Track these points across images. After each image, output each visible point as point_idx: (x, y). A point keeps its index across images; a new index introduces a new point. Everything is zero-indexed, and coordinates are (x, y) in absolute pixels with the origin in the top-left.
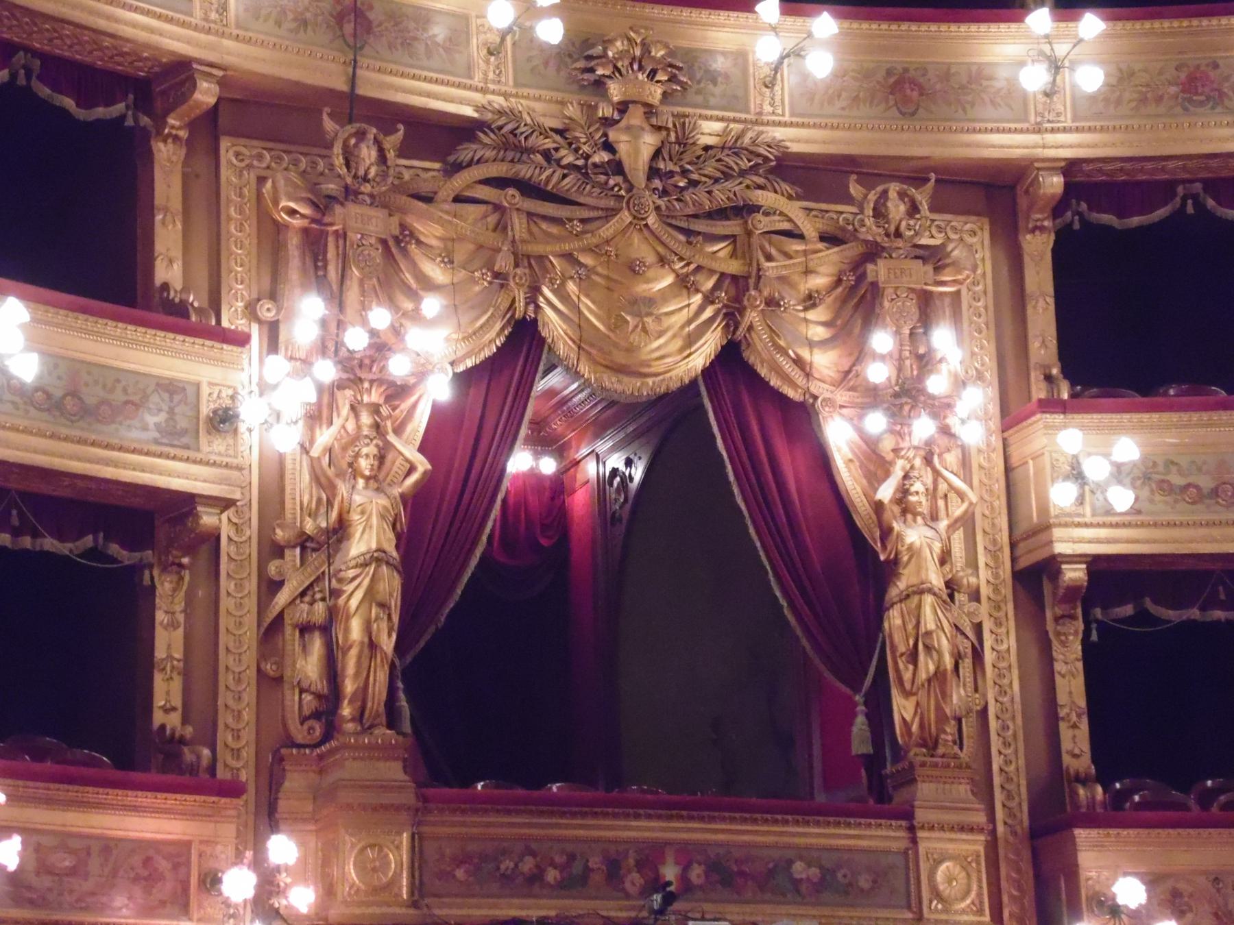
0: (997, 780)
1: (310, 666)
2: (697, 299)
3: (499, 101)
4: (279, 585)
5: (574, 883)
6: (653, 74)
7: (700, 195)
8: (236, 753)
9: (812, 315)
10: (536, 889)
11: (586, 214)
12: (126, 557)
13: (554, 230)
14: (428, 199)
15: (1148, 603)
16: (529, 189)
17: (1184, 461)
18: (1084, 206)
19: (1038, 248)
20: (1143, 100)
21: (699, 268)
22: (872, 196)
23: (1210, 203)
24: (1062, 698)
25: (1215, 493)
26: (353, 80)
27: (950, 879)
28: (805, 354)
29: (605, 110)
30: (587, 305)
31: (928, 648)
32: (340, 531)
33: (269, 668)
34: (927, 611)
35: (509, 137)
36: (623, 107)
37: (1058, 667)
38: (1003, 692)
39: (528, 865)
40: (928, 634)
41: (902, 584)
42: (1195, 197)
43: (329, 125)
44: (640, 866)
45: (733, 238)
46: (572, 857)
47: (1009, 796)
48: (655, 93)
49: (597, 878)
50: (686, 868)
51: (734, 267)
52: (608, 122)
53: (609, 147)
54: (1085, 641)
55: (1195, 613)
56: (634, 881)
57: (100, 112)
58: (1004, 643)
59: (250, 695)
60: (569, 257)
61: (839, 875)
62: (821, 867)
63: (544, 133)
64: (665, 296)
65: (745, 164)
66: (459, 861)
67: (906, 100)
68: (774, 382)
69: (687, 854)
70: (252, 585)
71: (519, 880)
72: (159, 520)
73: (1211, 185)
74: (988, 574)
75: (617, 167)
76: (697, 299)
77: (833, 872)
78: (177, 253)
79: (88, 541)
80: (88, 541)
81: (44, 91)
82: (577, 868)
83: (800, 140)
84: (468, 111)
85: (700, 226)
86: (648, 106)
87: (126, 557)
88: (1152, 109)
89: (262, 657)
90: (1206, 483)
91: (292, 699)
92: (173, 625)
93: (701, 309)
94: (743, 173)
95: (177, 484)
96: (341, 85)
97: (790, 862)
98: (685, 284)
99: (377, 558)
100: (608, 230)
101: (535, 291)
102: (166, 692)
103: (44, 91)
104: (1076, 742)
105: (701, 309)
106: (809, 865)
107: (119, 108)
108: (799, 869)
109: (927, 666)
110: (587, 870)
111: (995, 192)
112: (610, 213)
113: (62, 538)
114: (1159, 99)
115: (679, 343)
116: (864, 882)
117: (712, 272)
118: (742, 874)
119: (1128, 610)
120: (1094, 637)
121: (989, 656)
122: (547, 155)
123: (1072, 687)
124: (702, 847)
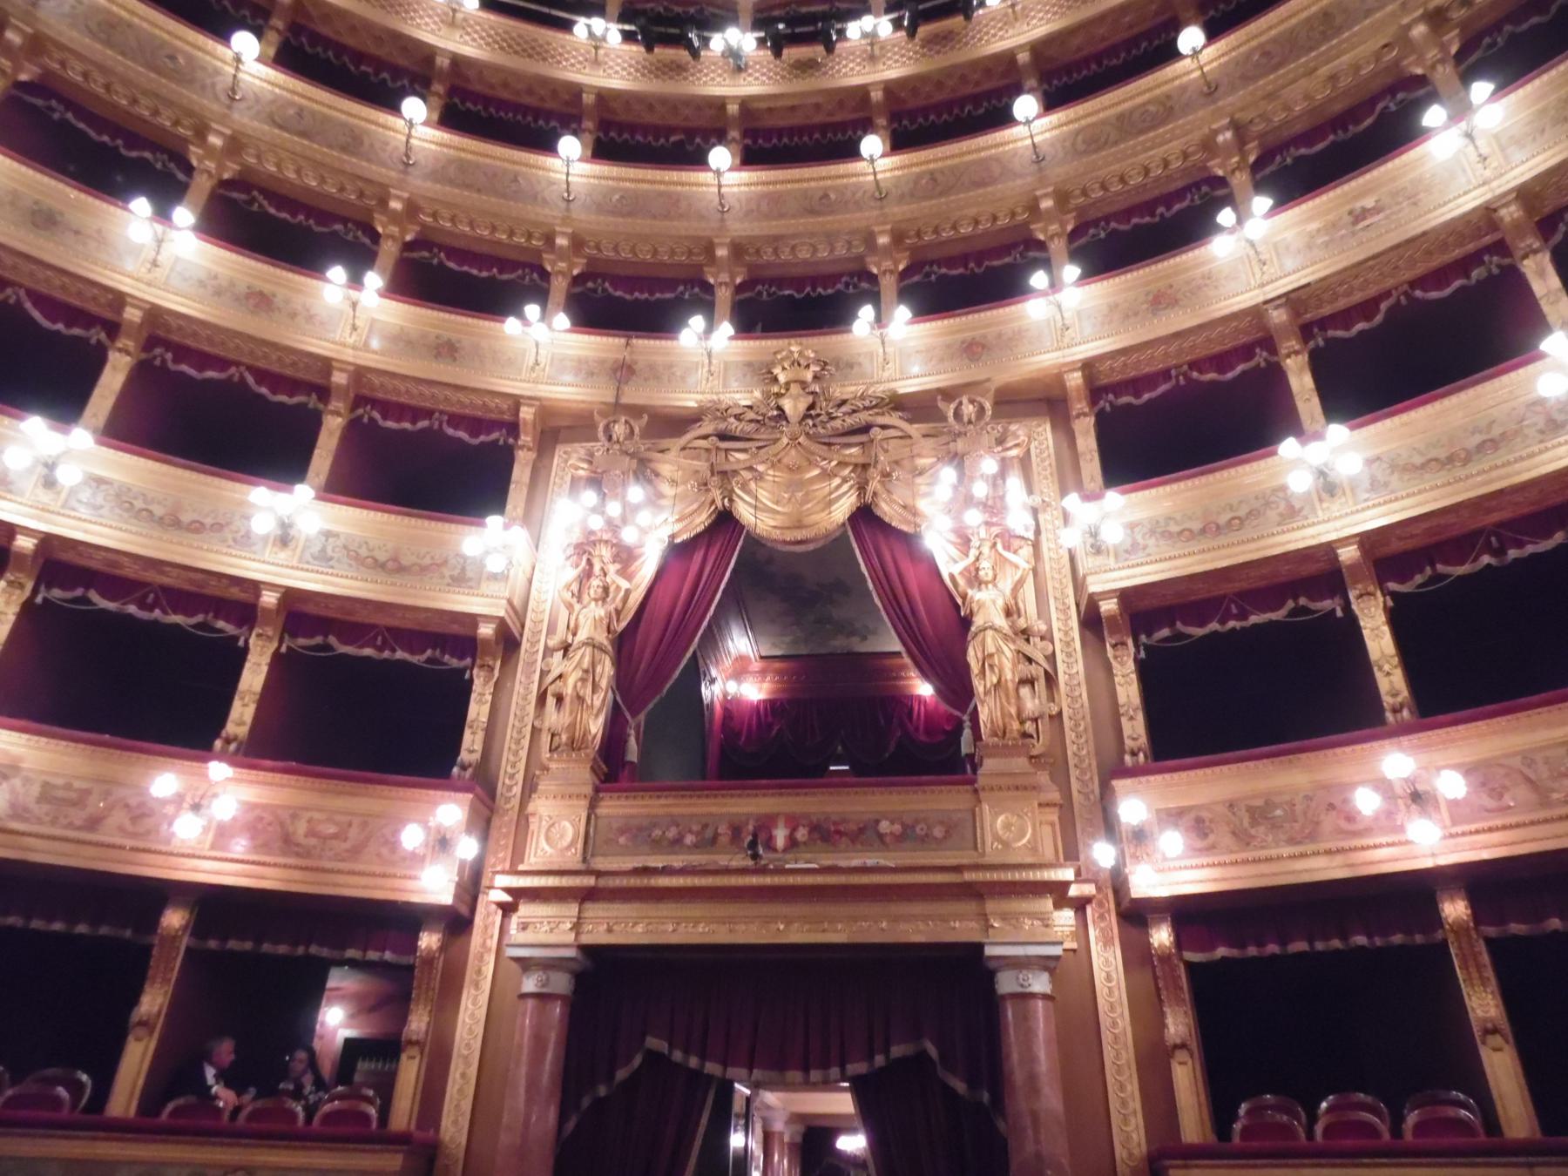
0: (1071, 762)
2: (837, 481)
5: (708, 842)
6: (808, 366)
7: (837, 424)
8: (512, 777)
12: (455, 663)
15: (1179, 625)
16: (723, 436)
17: (1178, 516)
18: (1111, 396)
20: (1127, 317)
21: (840, 463)
22: (953, 406)
23: (1195, 374)
24: (1122, 699)
25: (1203, 531)
27: (1007, 826)
29: (776, 389)
30: (764, 496)
31: (991, 666)
34: (989, 641)
35: (721, 412)
36: (788, 384)
39: (672, 833)
40: (991, 655)
46: (705, 826)
47: (1083, 772)
48: (809, 376)
49: (724, 840)
50: (794, 830)
51: (861, 460)
52: (779, 395)
53: (779, 408)
54: (1136, 660)
55: (1214, 626)
57: (482, 438)
58: (1072, 666)
60: (750, 469)
61: (918, 829)
62: (903, 824)
64: (812, 480)
66: (622, 831)
71: (665, 843)
73: (1193, 365)
74: (1065, 626)
75: (782, 415)
77: (913, 827)
81: (450, 431)
82: (709, 833)
83: (906, 387)
87: (455, 663)
89: (536, 717)
90: (1196, 526)
91: (545, 739)
92: (480, 702)
97: (877, 822)
98: (827, 475)
99: (591, 643)
103: (450, 431)
104: (1135, 729)
106: (892, 823)
107: (494, 436)
108: (884, 826)
109: (992, 679)
113: (412, 653)
114: (1136, 314)
115: (821, 506)
116: (938, 832)
118: (838, 832)
119: (1165, 632)
120: (1143, 655)
121: (1062, 678)
123: (1128, 691)
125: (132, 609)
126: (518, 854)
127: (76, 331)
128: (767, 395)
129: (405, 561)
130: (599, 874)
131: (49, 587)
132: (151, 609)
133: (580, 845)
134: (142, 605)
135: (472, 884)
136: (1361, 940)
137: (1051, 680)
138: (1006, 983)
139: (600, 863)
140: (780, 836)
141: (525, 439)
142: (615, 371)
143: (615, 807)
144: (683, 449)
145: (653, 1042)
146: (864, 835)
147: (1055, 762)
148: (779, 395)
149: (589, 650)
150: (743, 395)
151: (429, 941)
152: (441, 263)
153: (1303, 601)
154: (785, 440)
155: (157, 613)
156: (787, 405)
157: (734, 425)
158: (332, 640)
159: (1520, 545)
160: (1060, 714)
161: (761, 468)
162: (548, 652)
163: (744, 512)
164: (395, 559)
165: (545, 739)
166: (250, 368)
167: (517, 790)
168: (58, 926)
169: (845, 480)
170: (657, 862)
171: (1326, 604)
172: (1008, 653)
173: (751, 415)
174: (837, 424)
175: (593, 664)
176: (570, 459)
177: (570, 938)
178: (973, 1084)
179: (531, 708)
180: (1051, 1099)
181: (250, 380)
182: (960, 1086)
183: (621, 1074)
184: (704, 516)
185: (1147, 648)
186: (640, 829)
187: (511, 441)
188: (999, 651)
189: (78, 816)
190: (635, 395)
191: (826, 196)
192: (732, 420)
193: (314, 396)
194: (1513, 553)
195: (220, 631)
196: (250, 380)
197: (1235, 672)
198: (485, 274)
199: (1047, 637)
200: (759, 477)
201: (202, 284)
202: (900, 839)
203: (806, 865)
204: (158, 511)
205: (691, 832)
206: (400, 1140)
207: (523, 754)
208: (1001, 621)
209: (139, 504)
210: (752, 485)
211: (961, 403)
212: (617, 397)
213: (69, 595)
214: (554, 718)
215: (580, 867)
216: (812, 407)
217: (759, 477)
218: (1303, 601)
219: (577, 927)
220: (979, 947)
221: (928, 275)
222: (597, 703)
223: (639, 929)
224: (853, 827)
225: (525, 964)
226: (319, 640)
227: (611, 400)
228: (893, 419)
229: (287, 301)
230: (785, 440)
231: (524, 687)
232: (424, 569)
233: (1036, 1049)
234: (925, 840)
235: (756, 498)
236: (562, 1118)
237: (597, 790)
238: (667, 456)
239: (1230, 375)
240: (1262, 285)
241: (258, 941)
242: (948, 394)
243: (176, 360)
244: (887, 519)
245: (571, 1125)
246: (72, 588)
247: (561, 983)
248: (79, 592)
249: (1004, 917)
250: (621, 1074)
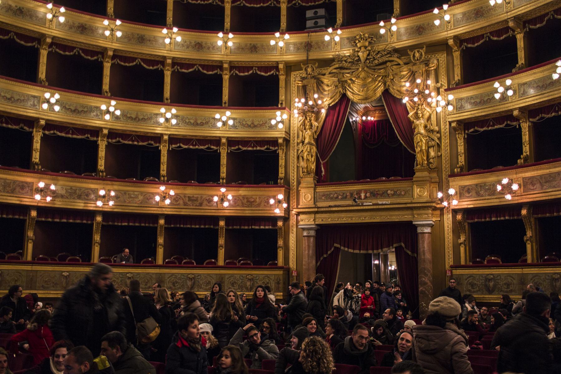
3: (337, 53)
5: (344, 198)
6: (366, 40)
7: (376, 62)
8: (293, 180)
12: (273, 148)
13: (348, 75)
14: (324, 75)
16: (341, 68)
19: (457, 55)
20: (468, 19)
24: (459, 151)
25: (480, 102)
27: (420, 191)
28: (399, 89)
29: (357, 50)
30: (355, 89)
36: (360, 48)
38: (446, 151)
39: (335, 196)
40: (419, 142)
42: (488, 37)
43: (302, 66)
44: (357, 194)
45: (384, 68)
48: (367, 44)
49: (348, 197)
50: (366, 194)
54: (464, 138)
55: (485, 129)
57: (269, 74)
58: (445, 142)
60: (351, 80)
63: (345, 56)
64: (369, 83)
65: (386, 53)
66: (323, 196)
67: (420, 31)
69: (366, 191)
75: (359, 60)
79: (266, 147)
80: (266, 147)
81: (259, 73)
82: (345, 195)
85: (375, 68)
87: (273, 148)
88: (469, 21)
91: (301, 169)
92: (282, 159)
93: (378, 84)
94: (386, 55)
98: (374, 80)
99: (309, 143)
102: (282, 171)
104: (462, 160)
105: (378, 84)
107: (272, 72)
108: (389, 192)
111: (441, 46)
113: (261, 147)
114: (470, 18)
116: (403, 193)
117: (380, 76)
119: (472, 130)
122: (345, 61)
123: (461, 148)
124: (369, 190)
125: (191, 147)
126: (298, 204)
127: (155, 67)
128: (354, 50)
129: (256, 123)
130: (318, 208)
131: (171, 145)
132: (195, 145)
133: (313, 200)
134: (193, 145)
135: (288, 211)
137: (439, 146)
138: (419, 230)
139: (320, 204)
140: (363, 195)
141: (281, 72)
142: (306, 46)
143: (320, 189)
144: (330, 73)
145: (336, 245)
146: (384, 194)
147: (438, 170)
148: (358, 52)
149: (309, 146)
150: (347, 52)
151: (280, 224)
152: (244, 5)
153: (509, 122)
154: (360, 69)
155: (197, 147)
156: (360, 54)
157: (345, 65)
158: (240, 147)
160: (441, 155)
161: (354, 79)
162: (298, 144)
163: (349, 94)
164: (253, 123)
165: (301, 169)
166: (200, 65)
167: (295, 183)
168: (197, 226)
169: (379, 82)
170: (332, 203)
171: (514, 123)
172: (424, 141)
173: (349, 60)
174: (376, 62)
175: (311, 150)
176: (296, 80)
177: (313, 223)
178: (413, 252)
179: (296, 160)
180: (428, 256)
181: (201, 69)
182: (410, 253)
183: (329, 252)
184: (338, 95)
185: (467, 134)
186: (327, 195)
187: (277, 73)
188: (421, 140)
189: (197, 203)
190: (314, 55)
192: (344, 62)
193: (219, 70)
195: (213, 149)
196: (201, 69)
197: (489, 144)
198: (258, 6)
199: (439, 132)
200: (353, 82)
201: (183, 46)
202: (393, 195)
203: (368, 204)
204: (192, 121)
206: (281, 268)
207: (295, 173)
208: (422, 131)
209: (187, 121)
210: (351, 85)
211: (415, 53)
212: (307, 57)
213: (176, 146)
214: (303, 164)
215: (313, 206)
216: (368, 55)
217: (353, 82)
218: (509, 122)
219: (314, 220)
220: (411, 222)
222: (313, 159)
223: (329, 220)
224: (381, 192)
225: (303, 229)
226: (237, 147)
227: (305, 58)
228: (395, 58)
229: (206, 44)
230: (360, 69)
231: (293, 154)
232: (261, 125)
233: (425, 245)
234: (400, 195)
235: (353, 90)
236: (317, 262)
237: (315, 185)
238: (325, 77)
239: (502, 38)
240: (507, 12)
241: (240, 226)
242: (412, 48)
243: (181, 68)
244: (393, 94)
245: (319, 264)
246: (177, 144)
247: (312, 233)
248: (178, 145)
249: (418, 215)
250: (329, 252)
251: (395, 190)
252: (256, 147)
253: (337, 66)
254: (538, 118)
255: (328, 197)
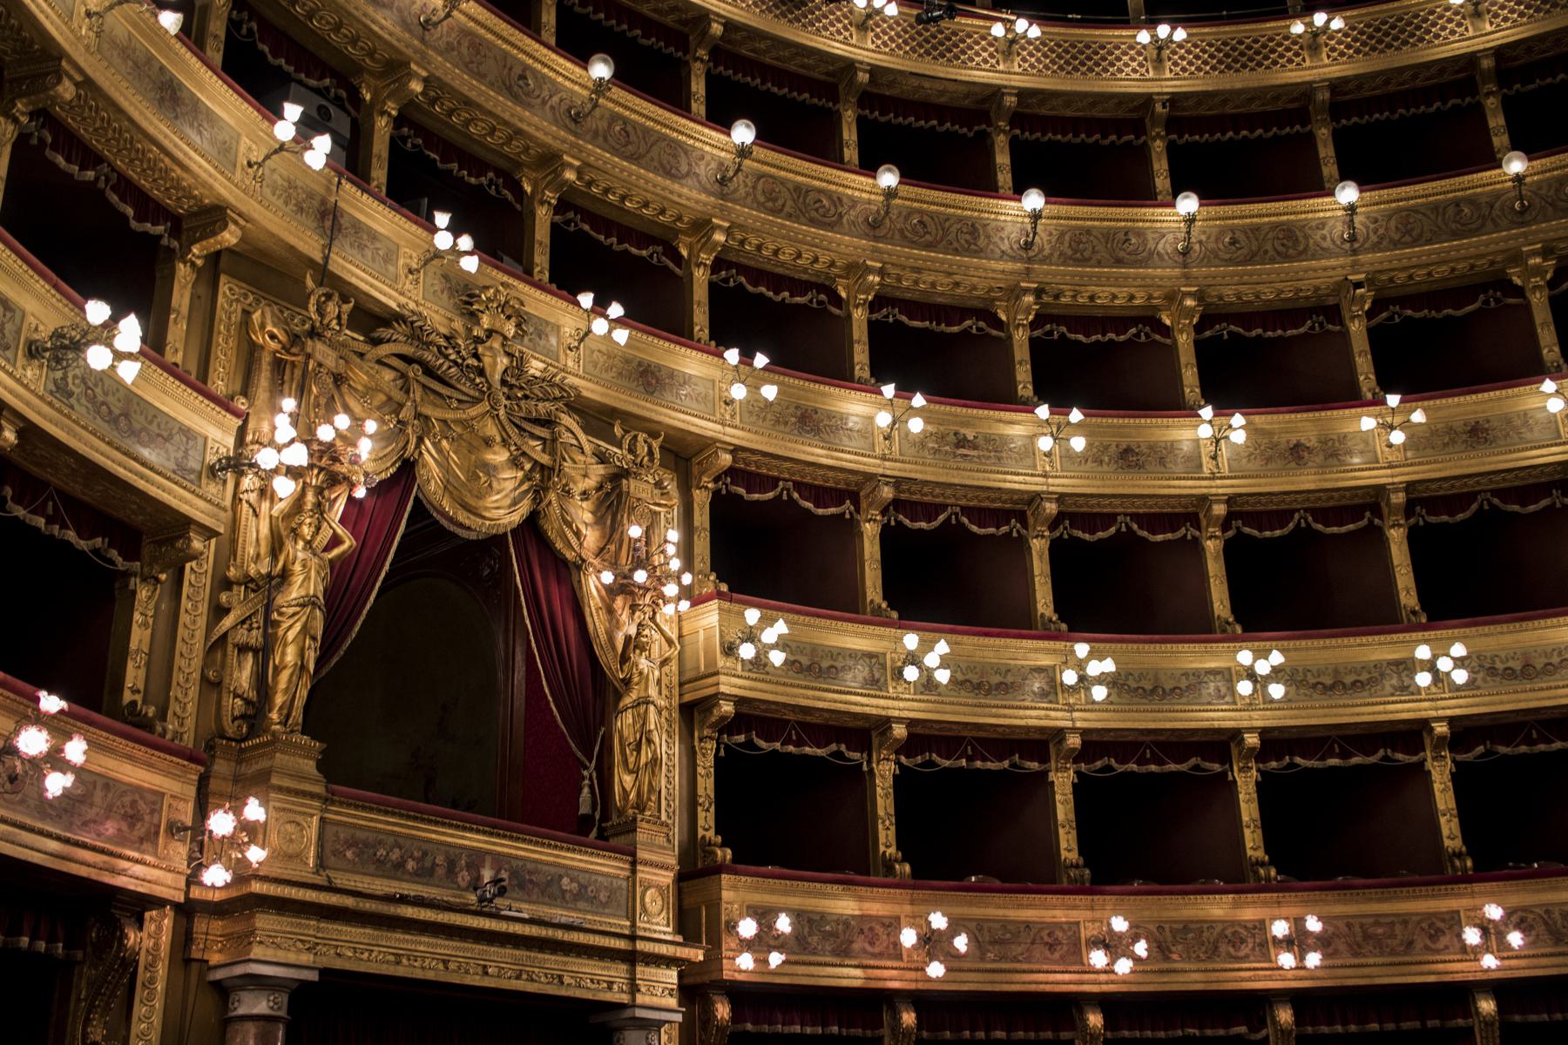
1: (243, 675)
3: (412, 305)
4: (227, 611)
5: (424, 874)
9: (584, 504)
10: (399, 874)
11: (461, 397)
16: (429, 371)
19: (701, 499)
20: (778, 421)
24: (700, 791)
26: (326, 258)
32: (285, 576)
33: (211, 674)
37: (700, 770)
39: (396, 855)
41: (634, 695)
43: (310, 283)
44: (469, 866)
45: (544, 440)
46: (425, 854)
49: (440, 871)
50: (498, 872)
51: (545, 459)
52: (478, 340)
53: (476, 356)
56: (464, 877)
59: (193, 692)
66: (352, 843)
67: (649, 384)
68: (559, 545)
70: (203, 608)
72: (155, 535)
75: (481, 372)
76: (520, 474)
78: (180, 345)
82: (428, 864)
84: (394, 305)
86: (505, 338)
88: (782, 427)
95: (185, 509)
96: (317, 256)
97: (561, 877)
100: (474, 411)
101: (420, 440)
102: (134, 675)
104: (706, 820)
107: (160, 229)
110: (434, 864)
112: (476, 401)
115: (508, 501)
116: (603, 896)
118: (531, 881)
119: (741, 738)
120: (722, 753)
123: (706, 786)
136: (835, 1029)
153: (843, 748)
159: (984, 759)
170: (382, 886)
171: (856, 755)
186: (366, 844)
191: (523, 77)
194: (979, 764)
197: (785, 792)
205: (411, 856)
221: (568, 223)
239: (820, 511)
251: (583, 878)
252: (64, 526)
253: (408, 350)
254: (919, 759)
255: (369, 854)
